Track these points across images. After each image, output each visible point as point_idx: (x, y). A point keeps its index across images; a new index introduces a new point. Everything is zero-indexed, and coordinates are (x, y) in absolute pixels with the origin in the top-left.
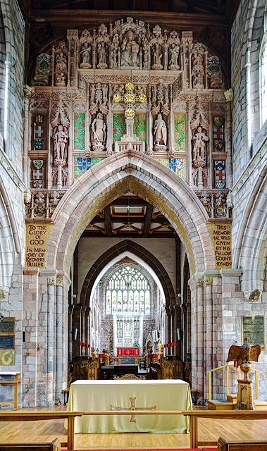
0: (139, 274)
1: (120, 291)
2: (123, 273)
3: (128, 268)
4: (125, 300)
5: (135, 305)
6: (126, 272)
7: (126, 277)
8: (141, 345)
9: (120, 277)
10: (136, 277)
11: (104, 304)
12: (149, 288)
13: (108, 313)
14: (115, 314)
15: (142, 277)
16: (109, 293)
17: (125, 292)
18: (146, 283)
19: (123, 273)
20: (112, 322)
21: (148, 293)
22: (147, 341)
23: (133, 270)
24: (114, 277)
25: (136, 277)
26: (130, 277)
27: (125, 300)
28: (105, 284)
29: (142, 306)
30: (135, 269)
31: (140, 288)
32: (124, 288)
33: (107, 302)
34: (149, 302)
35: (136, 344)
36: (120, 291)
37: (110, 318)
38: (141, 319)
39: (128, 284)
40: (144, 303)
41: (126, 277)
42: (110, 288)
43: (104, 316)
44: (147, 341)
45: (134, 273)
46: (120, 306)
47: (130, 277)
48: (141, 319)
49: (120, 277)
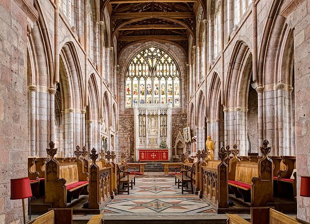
0: (166, 56)
1: (142, 79)
2: (146, 55)
3: (152, 49)
4: (149, 89)
5: (162, 96)
6: (150, 54)
7: (150, 61)
8: (169, 147)
9: (142, 60)
10: (163, 60)
11: (122, 94)
12: (178, 74)
13: (128, 106)
14: (136, 106)
15: (170, 60)
16: (128, 81)
17: (149, 81)
18: (175, 69)
19: (146, 55)
20: (132, 117)
21: (177, 81)
22: (177, 141)
23: (158, 51)
24: (135, 60)
25: (163, 60)
26: (155, 61)
27: (149, 89)
28: (124, 69)
29: (169, 96)
30: (161, 50)
31: (168, 74)
32: (147, 74)
33: (127, 93)
34: (178, 91)
35: (163, 145)
36: (142, 79)
37: (130, 112)
38: (169, 113)
39: (152, 69)
40: (172, 93)
41: (150, 61)
42: (130, 74)
43: (123, 109)
44: (177, 141)
45: (159, 55)
46: (142, 97)
47: (155, 61)
48: (169, 113)
49: (142, 60)
